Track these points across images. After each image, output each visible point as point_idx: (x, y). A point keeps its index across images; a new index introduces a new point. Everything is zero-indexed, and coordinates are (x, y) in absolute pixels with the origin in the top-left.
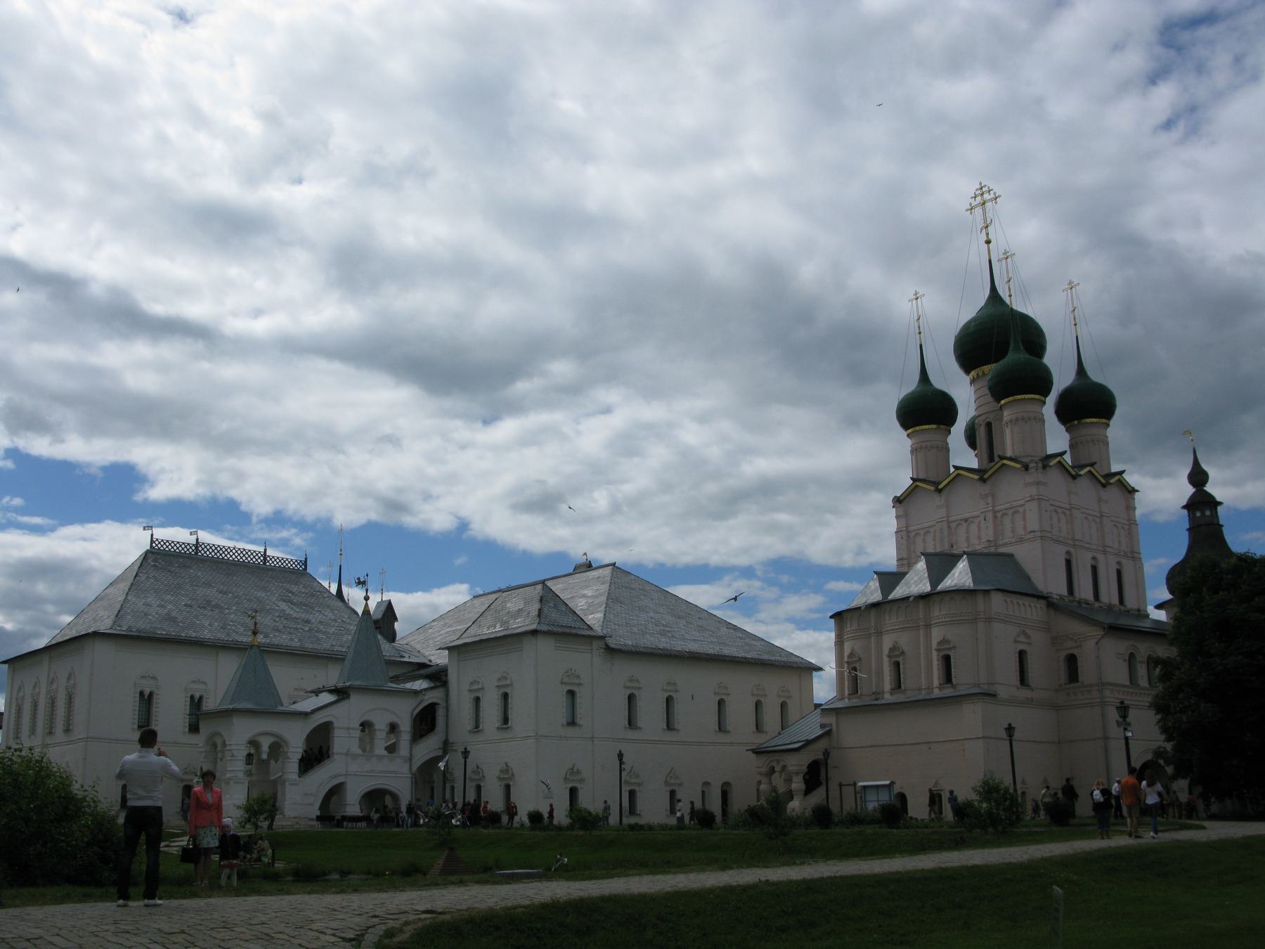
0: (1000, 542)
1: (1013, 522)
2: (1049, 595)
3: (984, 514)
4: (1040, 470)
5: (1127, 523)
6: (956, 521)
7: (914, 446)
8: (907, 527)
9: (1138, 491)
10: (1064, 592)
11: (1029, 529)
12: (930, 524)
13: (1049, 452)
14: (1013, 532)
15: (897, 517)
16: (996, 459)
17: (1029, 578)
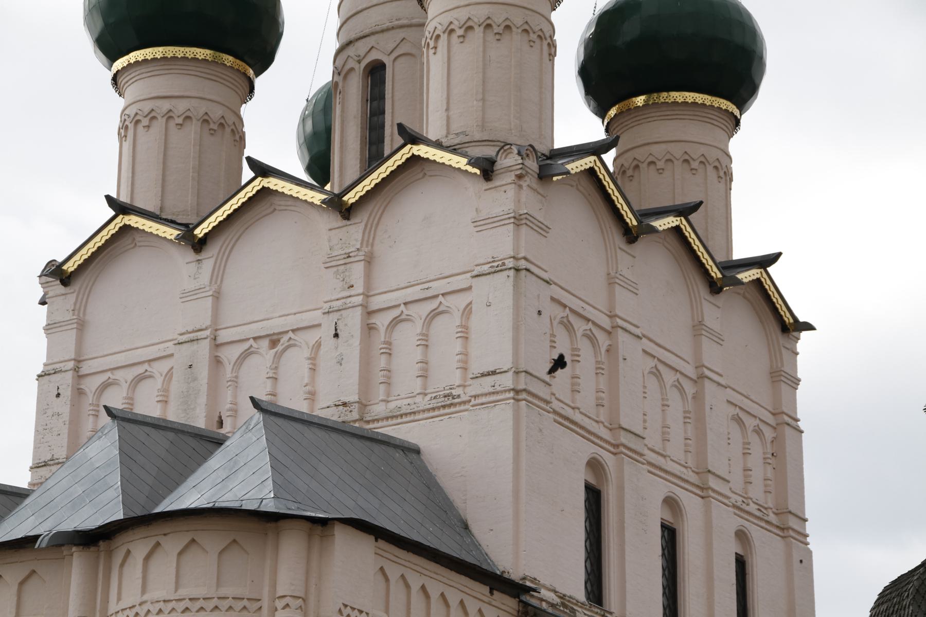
0: (379, 409)
1: (425, 343)
2: (528, 584)
3: (334, 317)
4: (530, 180)
5: (771, 419)
6: (248, 339)
7: (132, 111)
8: (78, 361)
9: (809, 327)
10: (576, 588)
11: (476, 367)
12: (153, 352)
13: (557, 145)
14: (424, 376)
15: (50, 328)
16: (391, 137)
17: (466, 527)
